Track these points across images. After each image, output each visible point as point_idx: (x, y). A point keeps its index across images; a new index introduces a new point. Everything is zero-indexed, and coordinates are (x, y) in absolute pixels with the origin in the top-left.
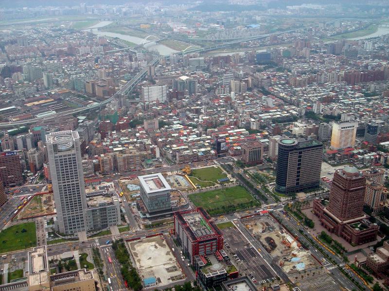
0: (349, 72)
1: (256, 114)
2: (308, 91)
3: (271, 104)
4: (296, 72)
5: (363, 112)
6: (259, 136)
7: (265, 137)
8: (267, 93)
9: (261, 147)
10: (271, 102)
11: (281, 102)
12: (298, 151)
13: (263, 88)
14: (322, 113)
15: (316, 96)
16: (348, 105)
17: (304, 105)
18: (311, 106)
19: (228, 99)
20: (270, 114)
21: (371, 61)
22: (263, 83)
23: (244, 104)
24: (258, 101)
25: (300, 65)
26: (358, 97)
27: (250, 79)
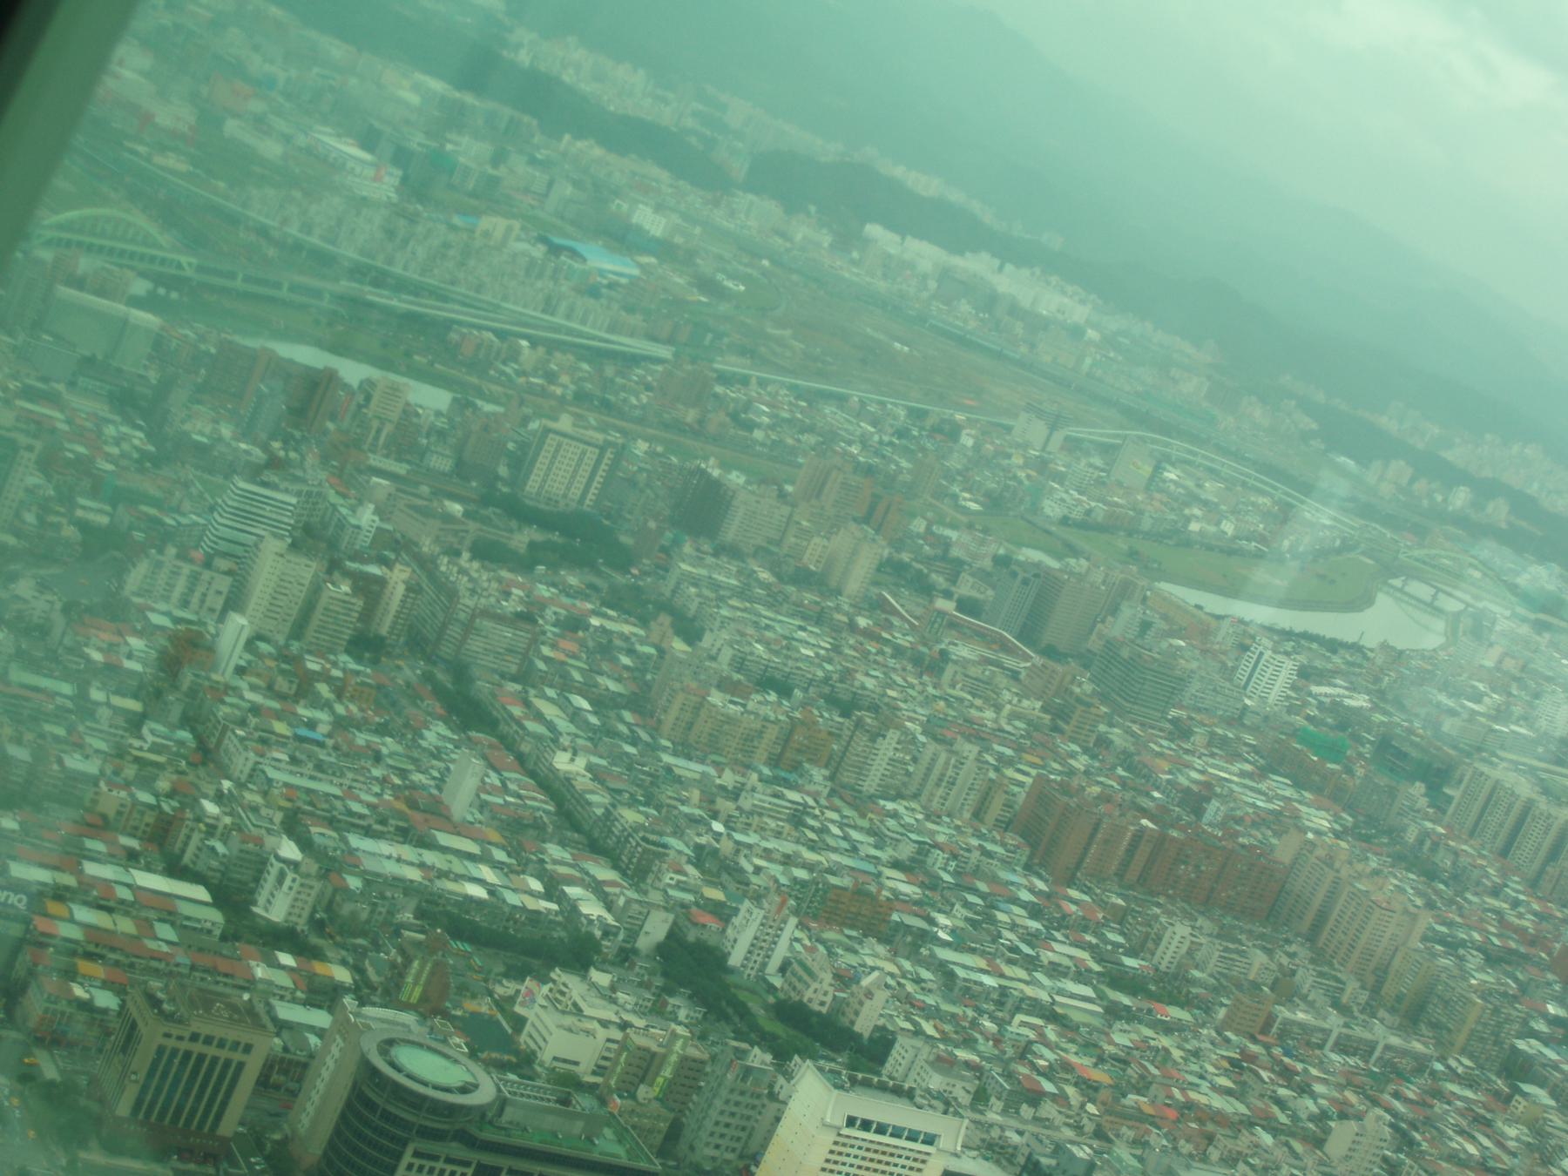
0: (1064, 788)
1: (332, 822)
2: (746, 802)
3: (460, 801)
4: (727, 655)
5: (1049, 1073)
6: (275, 971)
7: (323, 995)
8: (470, 714)
9: (248, 1049)
10: (468, 780)
11: (540, 804)
12: (476, 1157)
13: (460, 672)
14: (777, 982)
15: (788, 860)
16: (970, 994)
17: (679, 879)
18: (723, 913)
19: (184, 650)
20: (430, 857)
21: (1242, 774)
22: (475, 644)
23: (280, 727)
24: (389, 745)
25: (785, 624)
26: (1055, 971)
27: (398, 577)
